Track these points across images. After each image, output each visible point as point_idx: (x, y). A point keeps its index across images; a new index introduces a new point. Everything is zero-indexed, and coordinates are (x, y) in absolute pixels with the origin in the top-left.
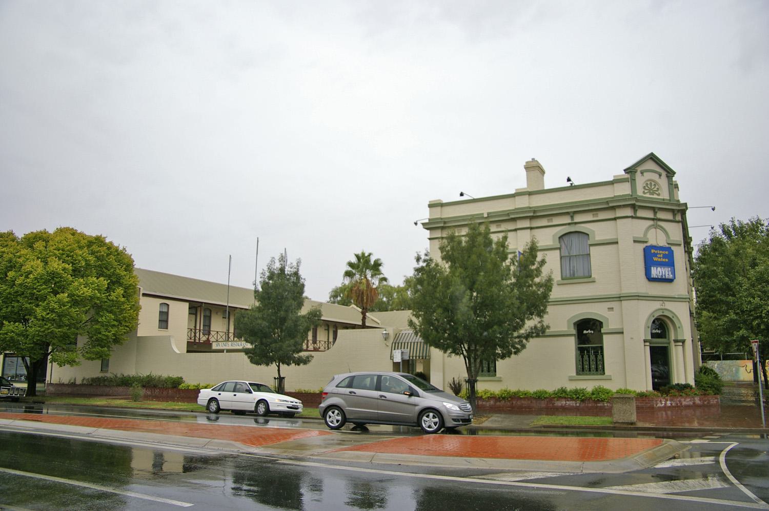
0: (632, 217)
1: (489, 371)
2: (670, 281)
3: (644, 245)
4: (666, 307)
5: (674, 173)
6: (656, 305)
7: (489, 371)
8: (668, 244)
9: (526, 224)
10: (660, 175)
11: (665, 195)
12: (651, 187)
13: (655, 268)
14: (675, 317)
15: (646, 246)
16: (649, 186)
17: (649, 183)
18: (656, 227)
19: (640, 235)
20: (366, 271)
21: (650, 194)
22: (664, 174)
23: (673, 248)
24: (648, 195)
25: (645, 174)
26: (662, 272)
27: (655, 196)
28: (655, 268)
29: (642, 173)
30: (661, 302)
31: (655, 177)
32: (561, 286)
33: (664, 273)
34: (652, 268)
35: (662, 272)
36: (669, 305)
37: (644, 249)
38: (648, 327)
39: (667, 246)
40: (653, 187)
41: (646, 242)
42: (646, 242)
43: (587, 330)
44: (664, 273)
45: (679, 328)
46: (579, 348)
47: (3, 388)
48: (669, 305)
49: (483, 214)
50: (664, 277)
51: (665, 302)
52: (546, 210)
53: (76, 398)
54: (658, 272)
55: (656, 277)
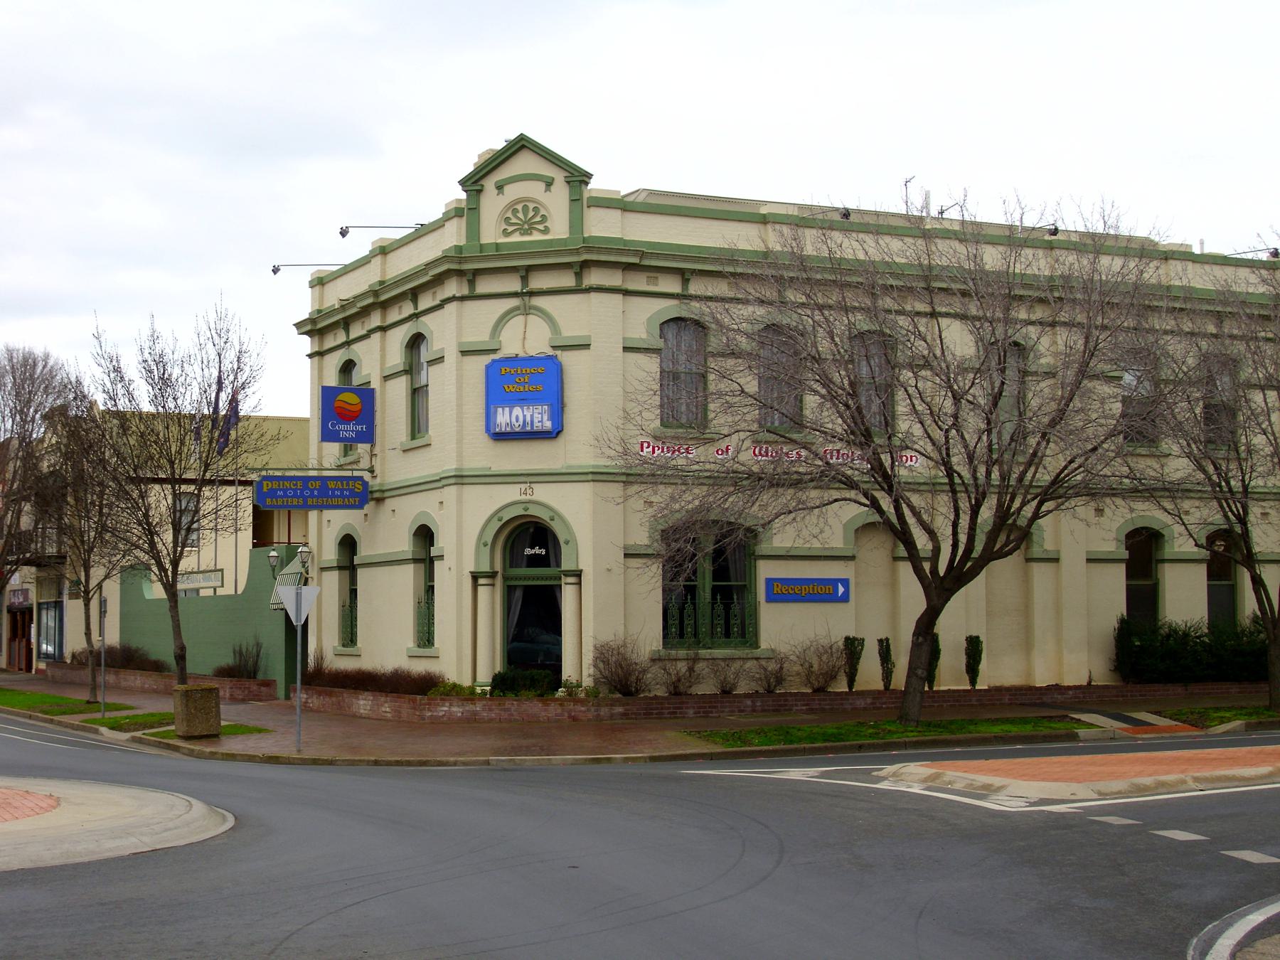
0: (462, 299)
1: (681, 635)
2: (553, 434)
3: (487, 359)
4: (534, 498)
5: (589, 176)
6: (511, 493)
7: (681, 635)
8: (554, 347)
9: (614, 279)
10: (549, 183)
11: (559, 229)
12: (528, 216)
13: (507, 410)
14: (556, 517)
15: (494, 361)
16: (521, 215)
17: (509, 214)
18: (526, 311)
19: (479, 336)
20: (1069, 325)
21: (522, 234)
22: (559, 176)
23: (566, 358)
24: (516, 238)
25: (507, 189)
26: (524, 416)
27: (537, 237)
28: (507, 410)
29: (500, 188)
30: (523, 486)
31: (534, 190)
32: (410, 454)
33: (528, 419)
34: (500, 410)
35: (524, 416)
36: (542, 493)
37: (488, 367)
38: (485, 545)
39: (551, 352)
40: (531, 214)
41: (494, 351)
42: (494, 351)
43: (532, 548)
44: (528, 419)
45: (567, 543)
46: (713, 586)
47: (101, 633)
48: (542, 493)
49: (334, 305)
50: (528, 428)
51: (533, 485)
52: (609, 251)
53: (350, 670)
54: (514, 420)
55: (509, 429)
